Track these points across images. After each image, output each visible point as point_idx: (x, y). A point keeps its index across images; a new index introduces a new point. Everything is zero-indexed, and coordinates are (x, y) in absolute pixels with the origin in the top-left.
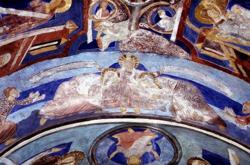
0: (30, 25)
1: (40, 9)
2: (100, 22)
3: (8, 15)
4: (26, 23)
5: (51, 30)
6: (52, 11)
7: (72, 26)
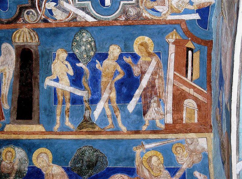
0: (160, 77)
1: (144, 66)
2: (171, 8)
3: (141, 97)
4: (156, 81)
5: (172, 57)
6: (150, 55)
7: (173, 36)
